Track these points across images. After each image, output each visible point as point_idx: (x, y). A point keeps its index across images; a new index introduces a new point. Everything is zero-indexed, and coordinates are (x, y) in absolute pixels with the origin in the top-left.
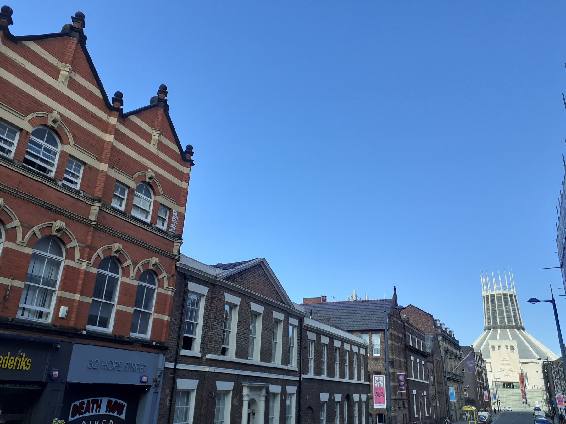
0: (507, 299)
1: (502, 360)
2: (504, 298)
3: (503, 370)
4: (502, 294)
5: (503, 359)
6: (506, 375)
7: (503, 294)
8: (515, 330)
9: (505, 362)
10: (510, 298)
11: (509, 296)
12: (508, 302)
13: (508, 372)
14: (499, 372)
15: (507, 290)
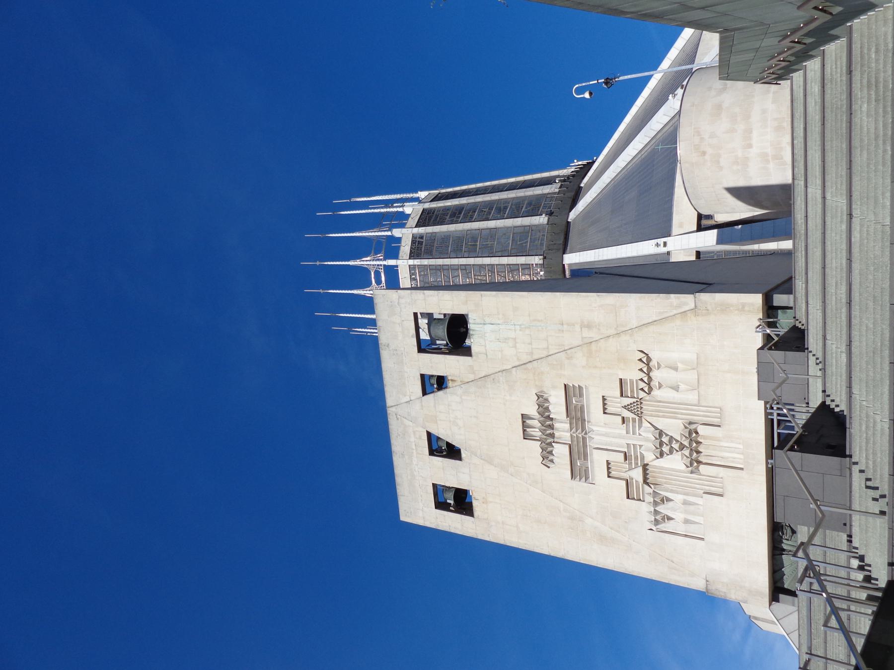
0: (433, 237)
1: (547, 456)
2: (429, 254)
3: (637, 475)
4: (411, 262)
5: (535, 447)
6: (695, 463)
7: (412, 256)
8: (572, 215)
9: (563, 429)
10: (434, 225)
11: (422, 230)
12: (445, 238)
13: (661, 424)
14: (659, 519)
15: (397, 233)
